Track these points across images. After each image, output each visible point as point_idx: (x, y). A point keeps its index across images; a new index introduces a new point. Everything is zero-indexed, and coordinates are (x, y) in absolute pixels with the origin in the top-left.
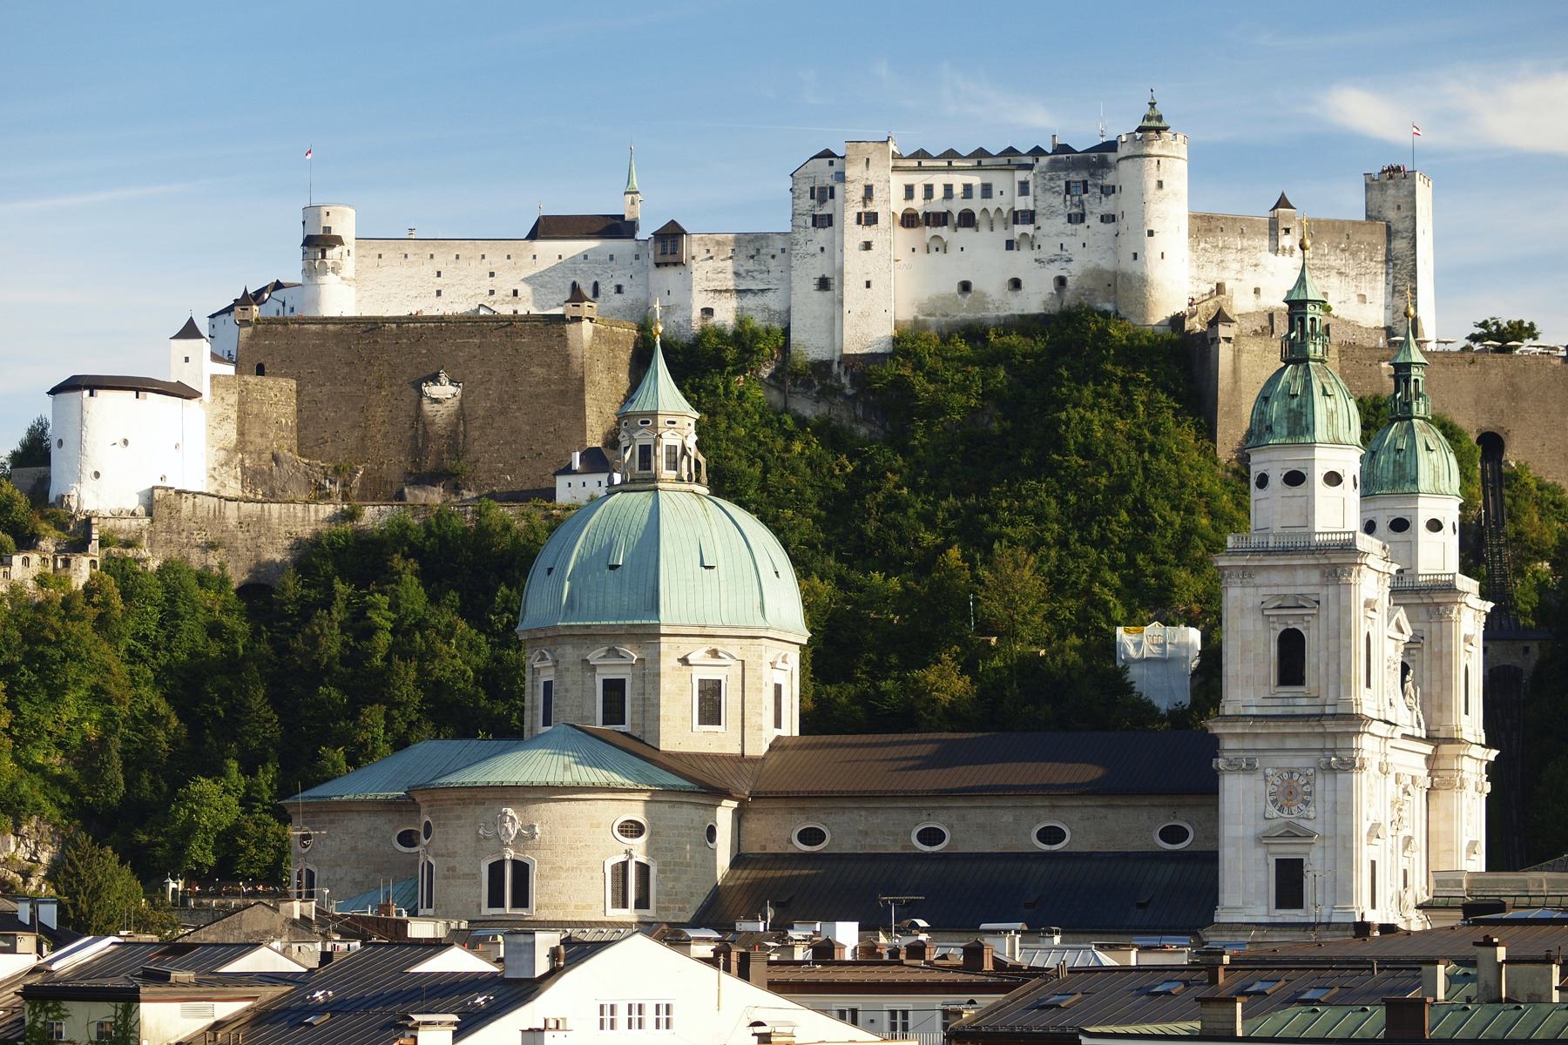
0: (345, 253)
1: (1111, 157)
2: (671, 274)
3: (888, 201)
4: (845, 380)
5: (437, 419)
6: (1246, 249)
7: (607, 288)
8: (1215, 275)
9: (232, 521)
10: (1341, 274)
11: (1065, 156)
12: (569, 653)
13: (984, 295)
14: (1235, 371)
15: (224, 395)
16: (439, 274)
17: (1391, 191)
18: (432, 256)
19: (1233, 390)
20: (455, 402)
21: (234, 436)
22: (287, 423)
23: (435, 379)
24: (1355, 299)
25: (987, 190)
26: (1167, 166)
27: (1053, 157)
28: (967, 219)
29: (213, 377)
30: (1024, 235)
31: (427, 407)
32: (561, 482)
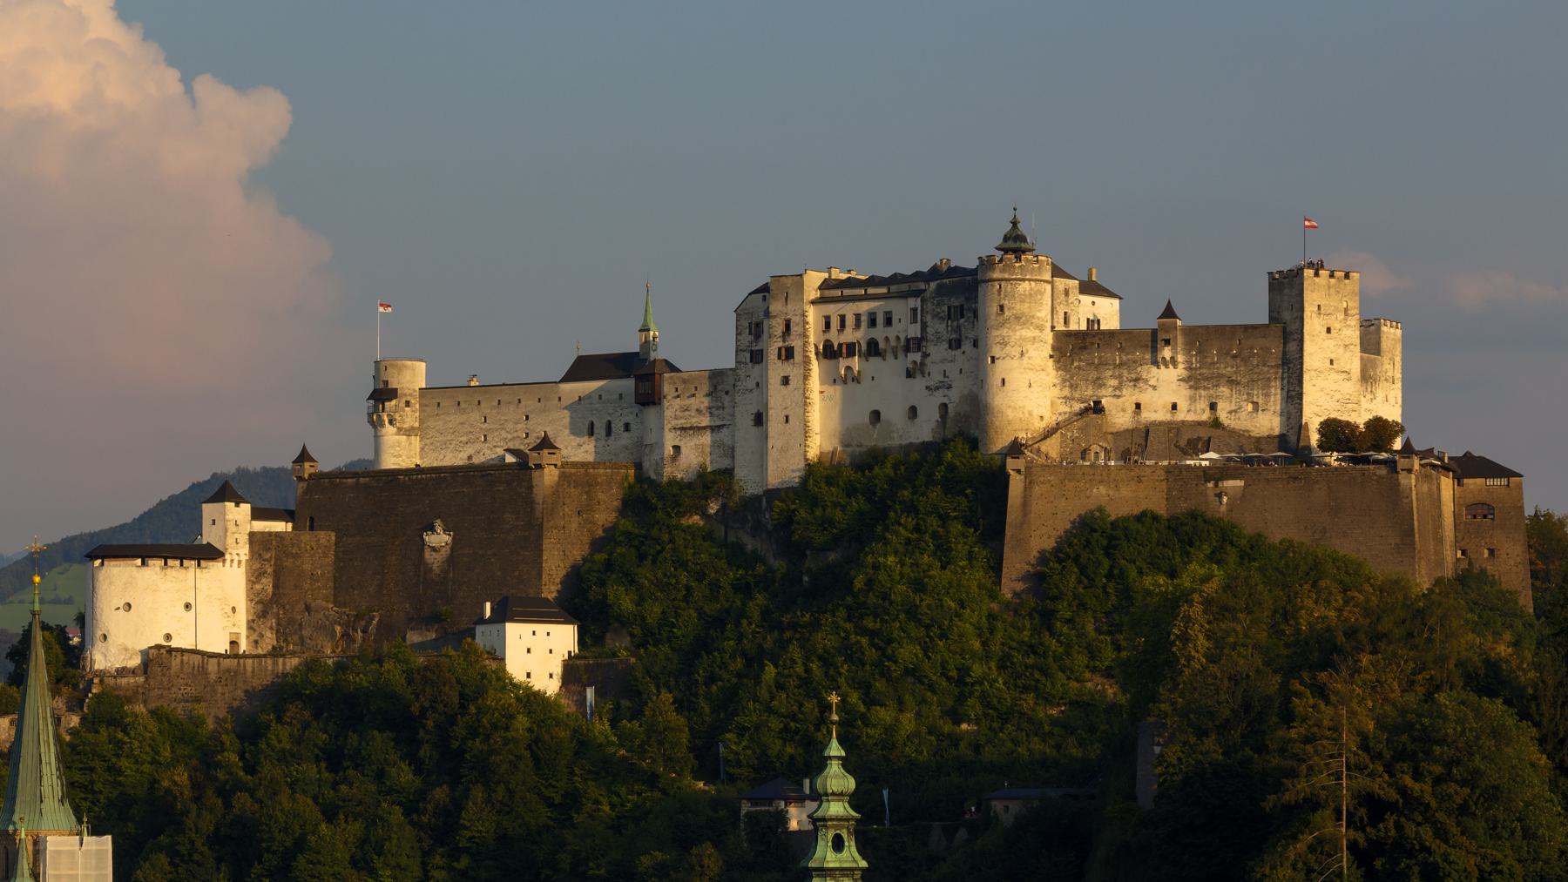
0: (403, 404)
3: (805, 335)
5: (435, 567)
6: (1125, 364)
7: (618, 426)
8: (1089, 392)
9: (213, 677)
10: (1231, 382)
11: (947, 280)
14: (1025, 503)
15: (261, 552)
17: (1286, 291)
18: (479, 402)
19: (1022, 524)
20: (448, 548)
21: (270, 590)
22: (323, 574)
23: (432, 529)
26: (1009, 290)
27: (939, 281)
29: (252, 535)
30: (915, 362)
31: (429, 556)
32: (479, 629)
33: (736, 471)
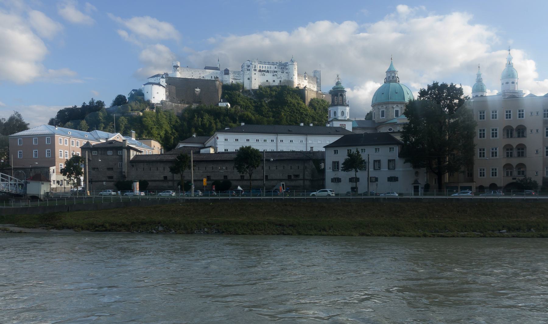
1: (287, 64)
2: (226, 76)
3: (258, 68)
4: (252, 93)
10: (312, 84)
12: (390, 106)
13: (269, 82)
16: (192, 73)
20: (200, 92)
21: (168, 94)
23: (197, 88)
24: (313, 87)
25: (270, 67)
28: (268, 72)
30: (275, 74)
31: (195, 92)
33: (245, 86)
